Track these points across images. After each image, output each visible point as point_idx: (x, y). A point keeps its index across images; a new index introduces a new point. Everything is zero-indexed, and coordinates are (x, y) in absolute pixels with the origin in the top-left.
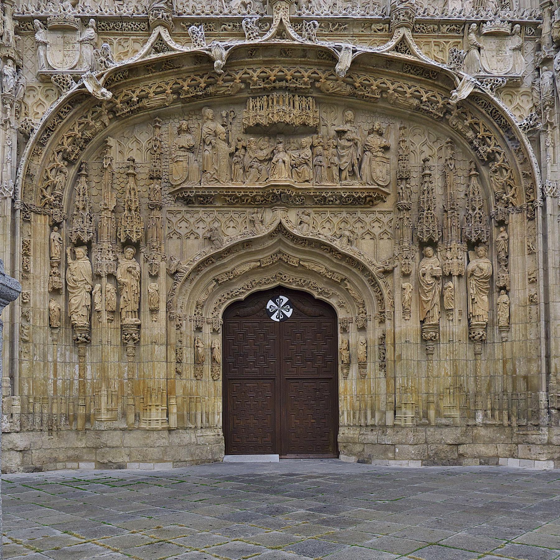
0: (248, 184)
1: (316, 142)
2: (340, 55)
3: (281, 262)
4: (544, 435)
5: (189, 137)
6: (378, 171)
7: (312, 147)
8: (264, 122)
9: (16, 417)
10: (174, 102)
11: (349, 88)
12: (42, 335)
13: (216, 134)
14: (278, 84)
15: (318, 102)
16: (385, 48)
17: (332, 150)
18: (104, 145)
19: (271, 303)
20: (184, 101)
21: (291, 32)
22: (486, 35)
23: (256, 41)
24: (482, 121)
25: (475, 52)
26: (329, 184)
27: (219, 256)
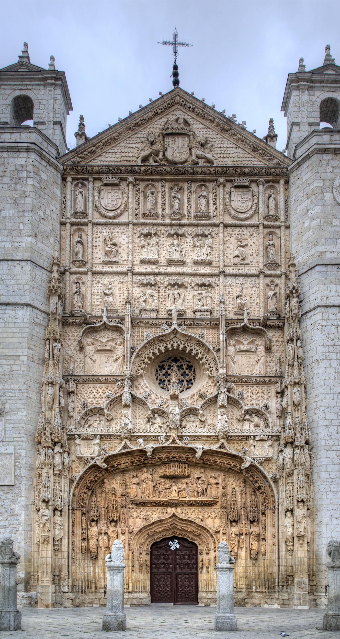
0: (161, 498)
1: (189, 481)
2: (197, 450)
3: (174, 527)
4: (276, 595)
5: (137, 479)
6: (214, 493)
7: (187, 483)
8: (167, 474)
9: (70, 587)
10: (131, 466)
11: (202, 461)
12: (79, 556)
14: (173, 459)
15: (189, 465)
16: (215, 447)
17: (195, 485)
18: (103, 482)
19: (170, 542)
20: (135, 466)
21: (178, 441)
23: (164, 445)
24: (255, 474)
25: (252, 447)
26: (193, 499)
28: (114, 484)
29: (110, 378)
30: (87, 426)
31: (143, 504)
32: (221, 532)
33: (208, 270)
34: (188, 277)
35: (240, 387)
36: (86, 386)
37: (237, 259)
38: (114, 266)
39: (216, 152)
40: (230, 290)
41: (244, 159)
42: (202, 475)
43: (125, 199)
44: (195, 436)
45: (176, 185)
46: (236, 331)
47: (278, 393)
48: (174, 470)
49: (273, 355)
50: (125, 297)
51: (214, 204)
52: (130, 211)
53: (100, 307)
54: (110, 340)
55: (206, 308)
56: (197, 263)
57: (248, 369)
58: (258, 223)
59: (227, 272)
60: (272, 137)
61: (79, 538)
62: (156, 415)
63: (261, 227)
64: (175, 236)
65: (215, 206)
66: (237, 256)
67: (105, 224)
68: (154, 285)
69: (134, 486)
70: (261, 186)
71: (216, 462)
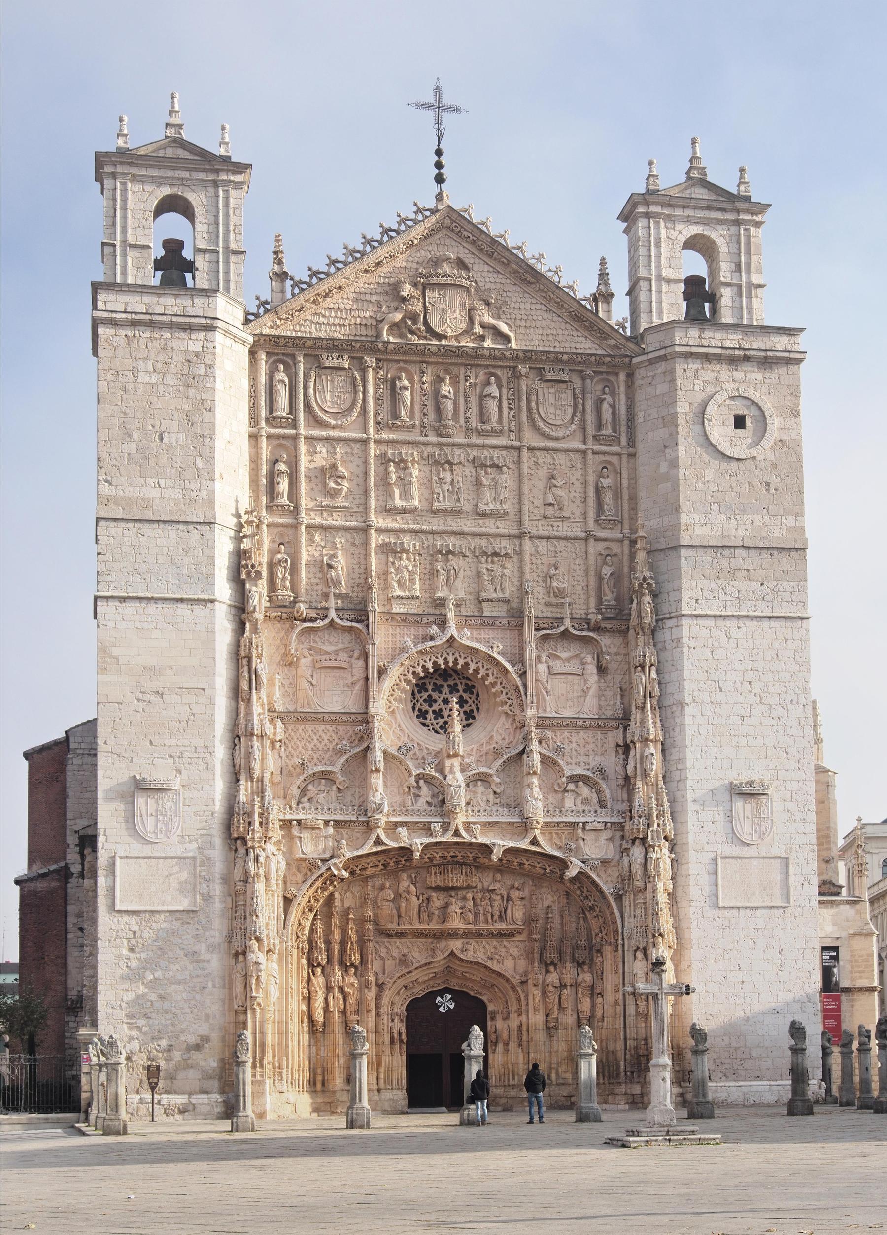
4: (622, 1089)
8: (441, 884)
13: (408, 892)
21: (463, 832)
26: (485, 926)
27: (410, 972)
29: (343, 716)
30: (305, 799)
31: (401, 935)
32: (530, 982)
33: (503, 527)
34: (469, 537)
35: (559, 734)
36: (301, 728)
37: (551, 507)
39: (513, 316)
40: (539, 562)
41: (560, 332)
43: (361, 395)
44: (490, 823)
47: (618, 745)
49: (609, 677)
50: (362, 571)
51: (511, 409)
53: (319, 588)
55: (500, 595)
58: (584, 447)
59: (534, 532)
60: (604, 296)
62: (421, 782)
64: (447, 466)
65: (512, 413)
66: (551, 504)
70: (588, 381)
71: (521, 864)
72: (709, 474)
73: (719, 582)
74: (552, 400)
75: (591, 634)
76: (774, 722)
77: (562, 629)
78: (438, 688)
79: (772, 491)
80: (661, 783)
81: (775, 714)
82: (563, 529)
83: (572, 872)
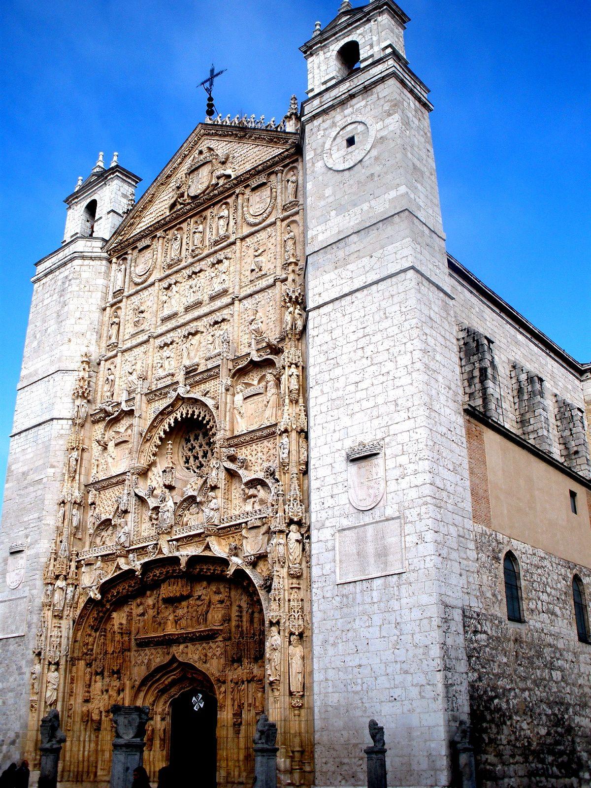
5: (141, 607)
18: (109, 618)
22: (250, 528)
26: (190, 630)
28: (119, 618)
33: (226, 300)
38: (140, 336)
42: (204, 592)
44: (185, 537)
45: (201, 216)
46: (244, 370)
48: (167, 590)
52: (158, 267)
54: (127, 428)
56: (212, 298)
57: (257, 419)
61: (80, 700)
63: (278, 223)
66: (253, 270)
67: (137, 292)
68: (172, 343)
69: (138, 618)
72: (328, 192)
73: (336, 271)
74: (258, 199)
75: (269, 357)
76: (384, 378)
77: (249, 359)
78: (196, 438)
79: (376, 178)
80: (294, 470)
81: (384, 371)
82: (263, 283)
83: (231, 571)
